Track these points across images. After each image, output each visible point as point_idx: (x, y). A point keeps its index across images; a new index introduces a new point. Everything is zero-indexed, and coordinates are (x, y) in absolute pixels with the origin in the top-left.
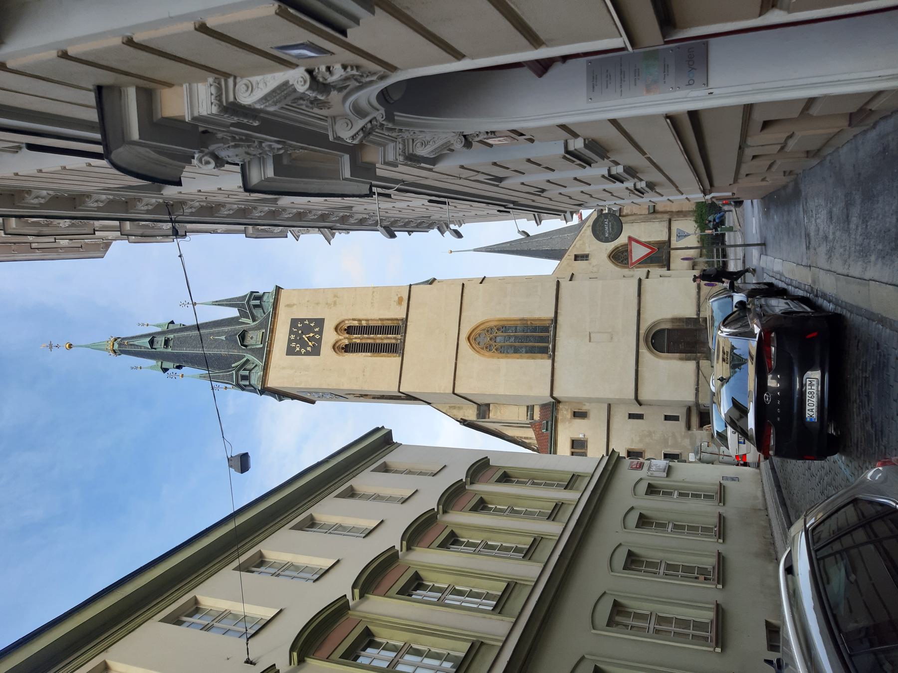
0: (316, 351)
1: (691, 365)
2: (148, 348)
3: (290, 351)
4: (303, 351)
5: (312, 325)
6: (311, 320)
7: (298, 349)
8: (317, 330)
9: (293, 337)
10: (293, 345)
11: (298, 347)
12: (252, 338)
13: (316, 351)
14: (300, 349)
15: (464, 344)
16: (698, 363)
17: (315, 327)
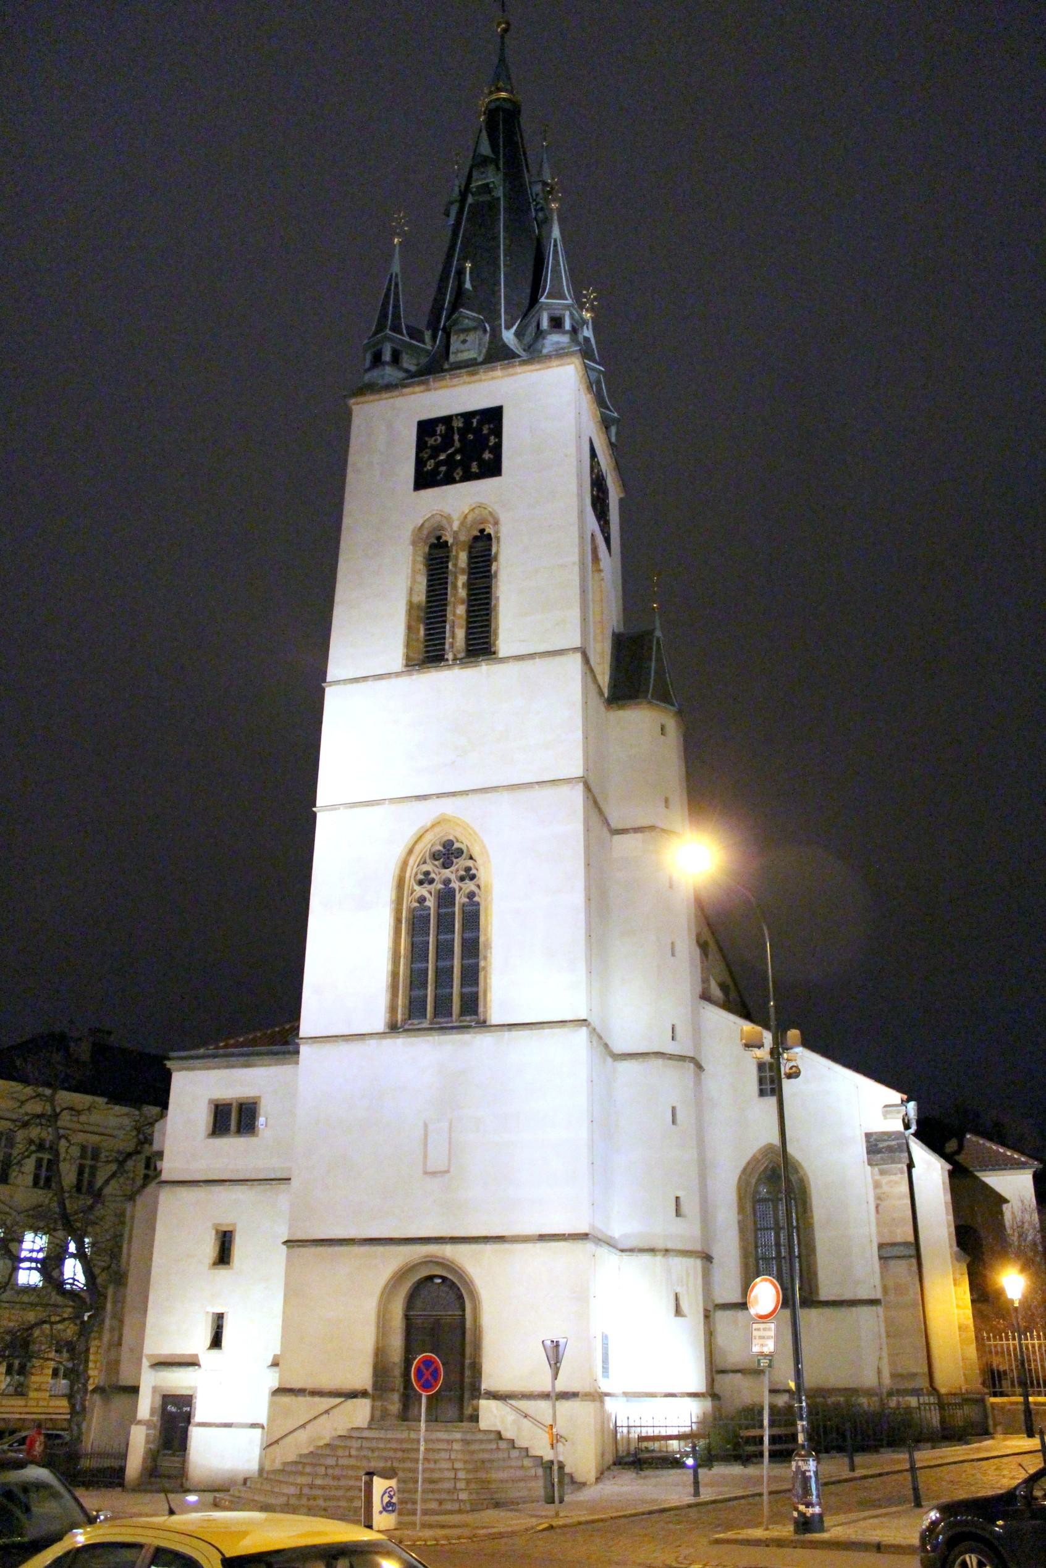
1: (362, 1376)
3: (426, 428)
4: (425, 455)
5: (487, 456)
6: (497, 450)
10: (441, 429)
12: (464, 342)
15: (427, 813)
16: (364, 1394)
17: (482, 463)
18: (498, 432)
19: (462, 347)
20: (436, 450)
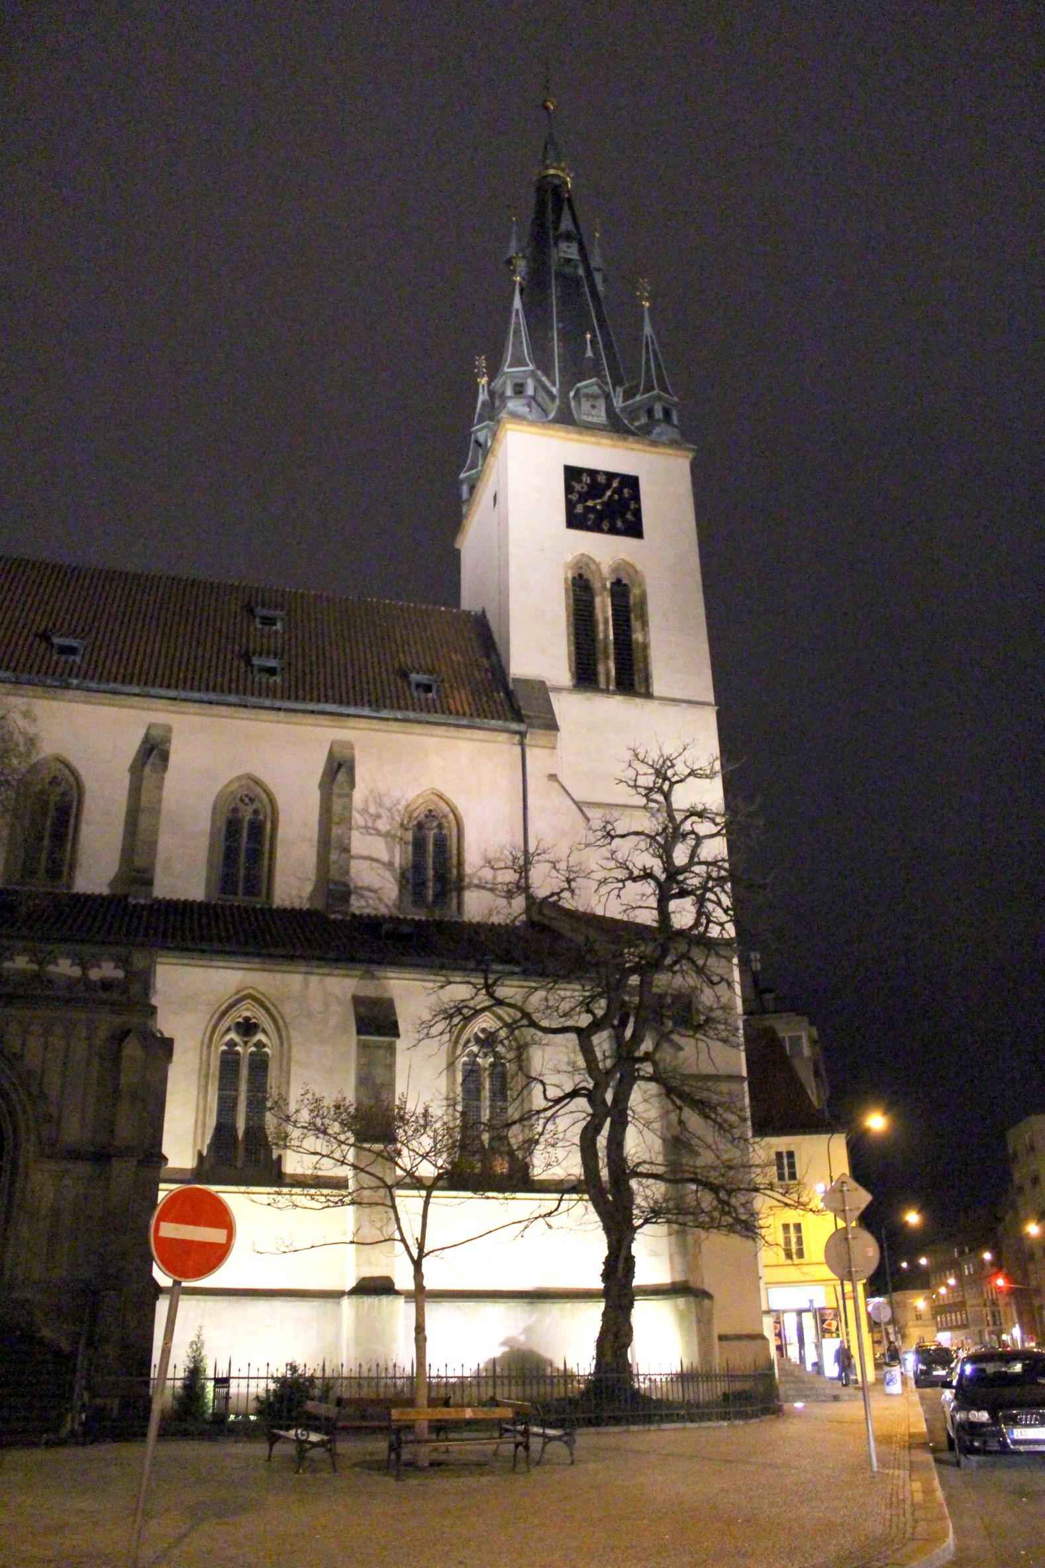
0: (574, 521)
2: (556, 229)
3: (572, 474)
4: (574, 497)
5: (629, 516)
6: (638, 513)
7: (577, 487)
8: (619, 524)
9: (602, 479)
10: (586, 479)
11: (582, 488)
12: (593, 407)
13: (574, 521)
14: (578, 492)
17: (625, 521)
18: (636, 497)
19: (594, 412)
20: (583, 498)
